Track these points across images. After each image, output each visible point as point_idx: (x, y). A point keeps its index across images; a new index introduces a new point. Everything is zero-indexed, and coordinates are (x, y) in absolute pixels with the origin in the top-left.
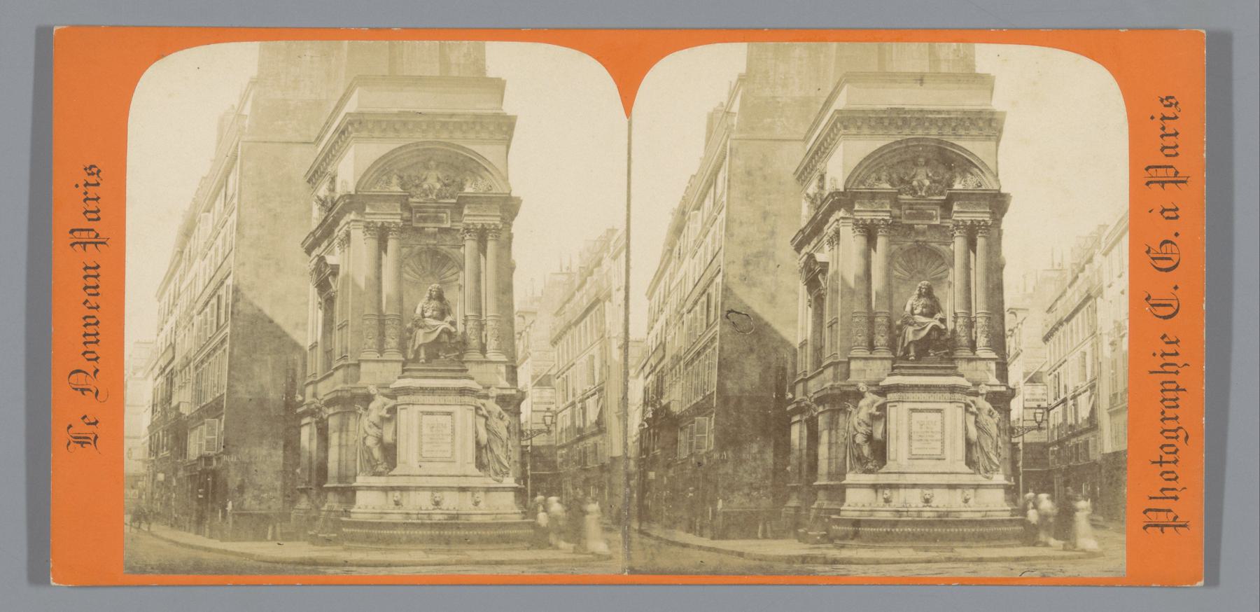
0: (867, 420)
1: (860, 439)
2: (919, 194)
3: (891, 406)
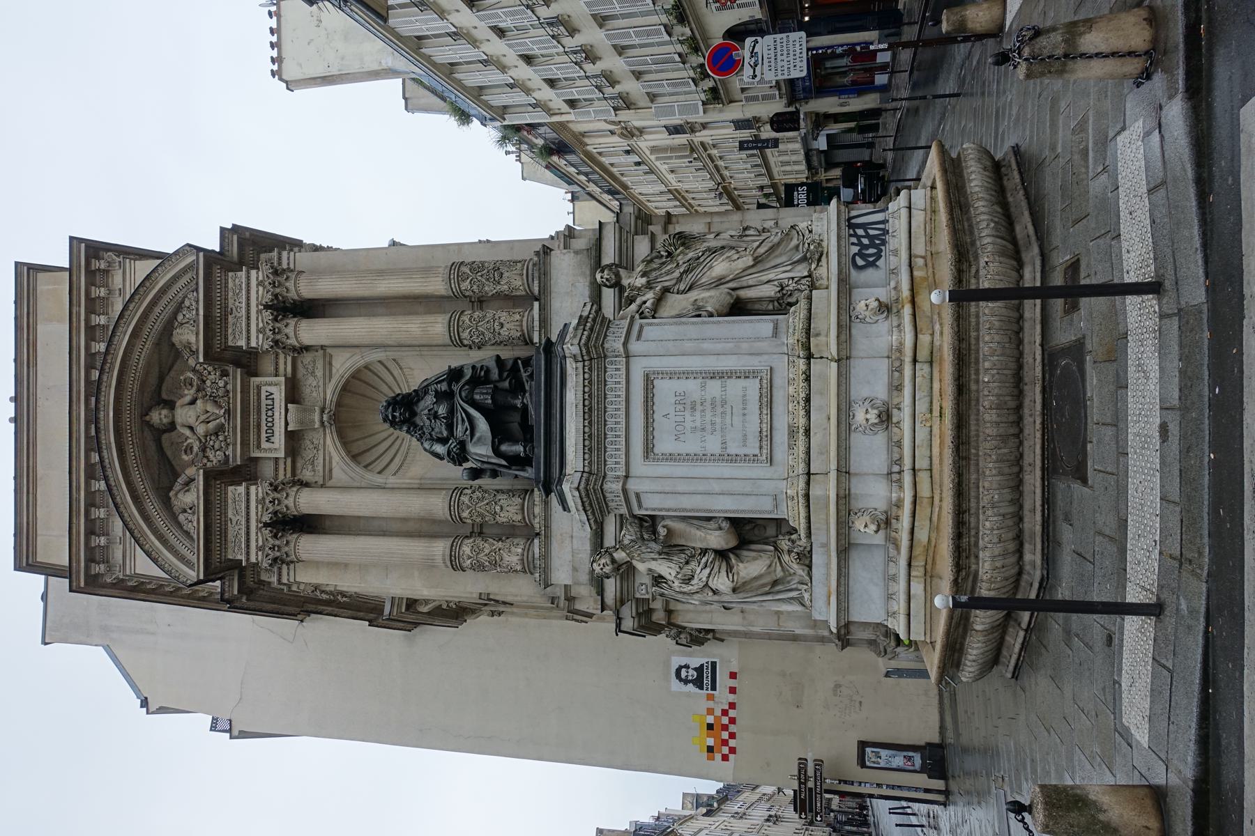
1: (722, 582)
2: (223, 421)
3: (640, 506)
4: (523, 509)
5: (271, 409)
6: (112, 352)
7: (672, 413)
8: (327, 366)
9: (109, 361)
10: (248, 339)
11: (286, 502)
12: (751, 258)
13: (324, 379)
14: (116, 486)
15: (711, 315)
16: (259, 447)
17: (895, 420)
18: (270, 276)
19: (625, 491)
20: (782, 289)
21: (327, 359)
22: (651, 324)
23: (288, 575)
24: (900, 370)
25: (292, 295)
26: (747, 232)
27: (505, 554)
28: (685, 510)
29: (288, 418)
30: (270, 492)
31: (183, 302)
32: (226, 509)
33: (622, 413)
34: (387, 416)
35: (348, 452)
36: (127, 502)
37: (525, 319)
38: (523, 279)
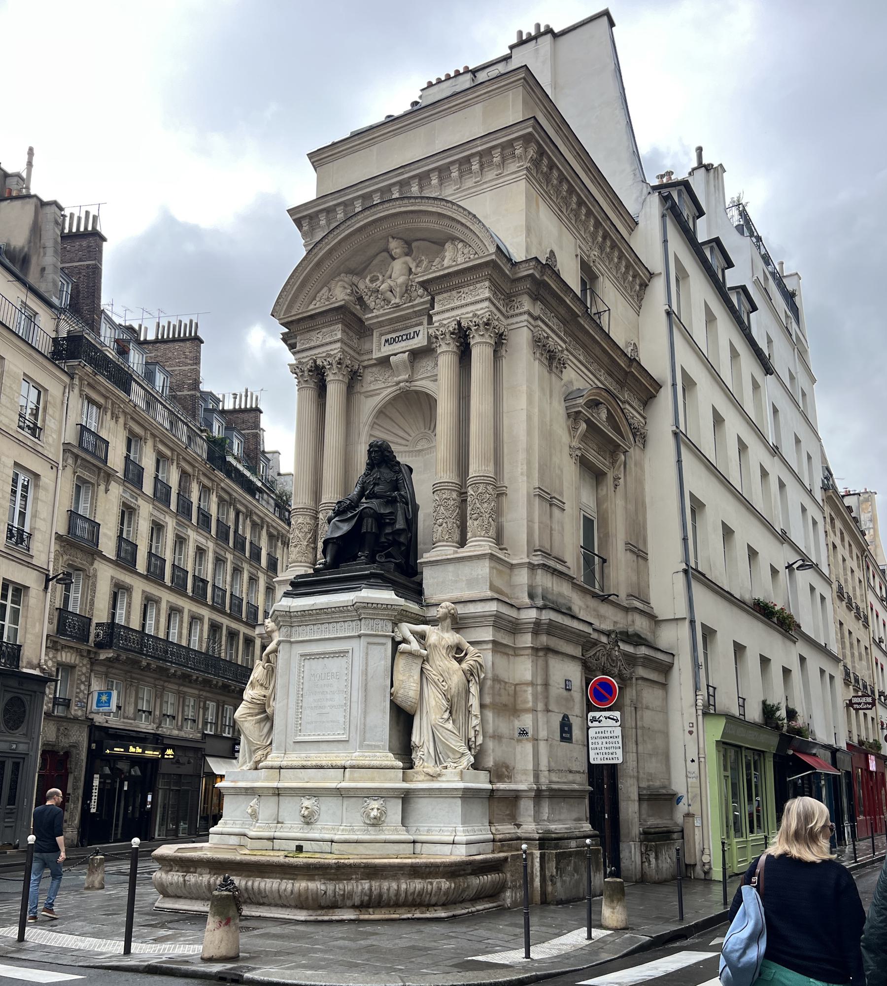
5: (407, 338)
11: (330, 374)
16: (382, 335)
32: (327, 326)
35: (385, 406)
37: (445, 543)
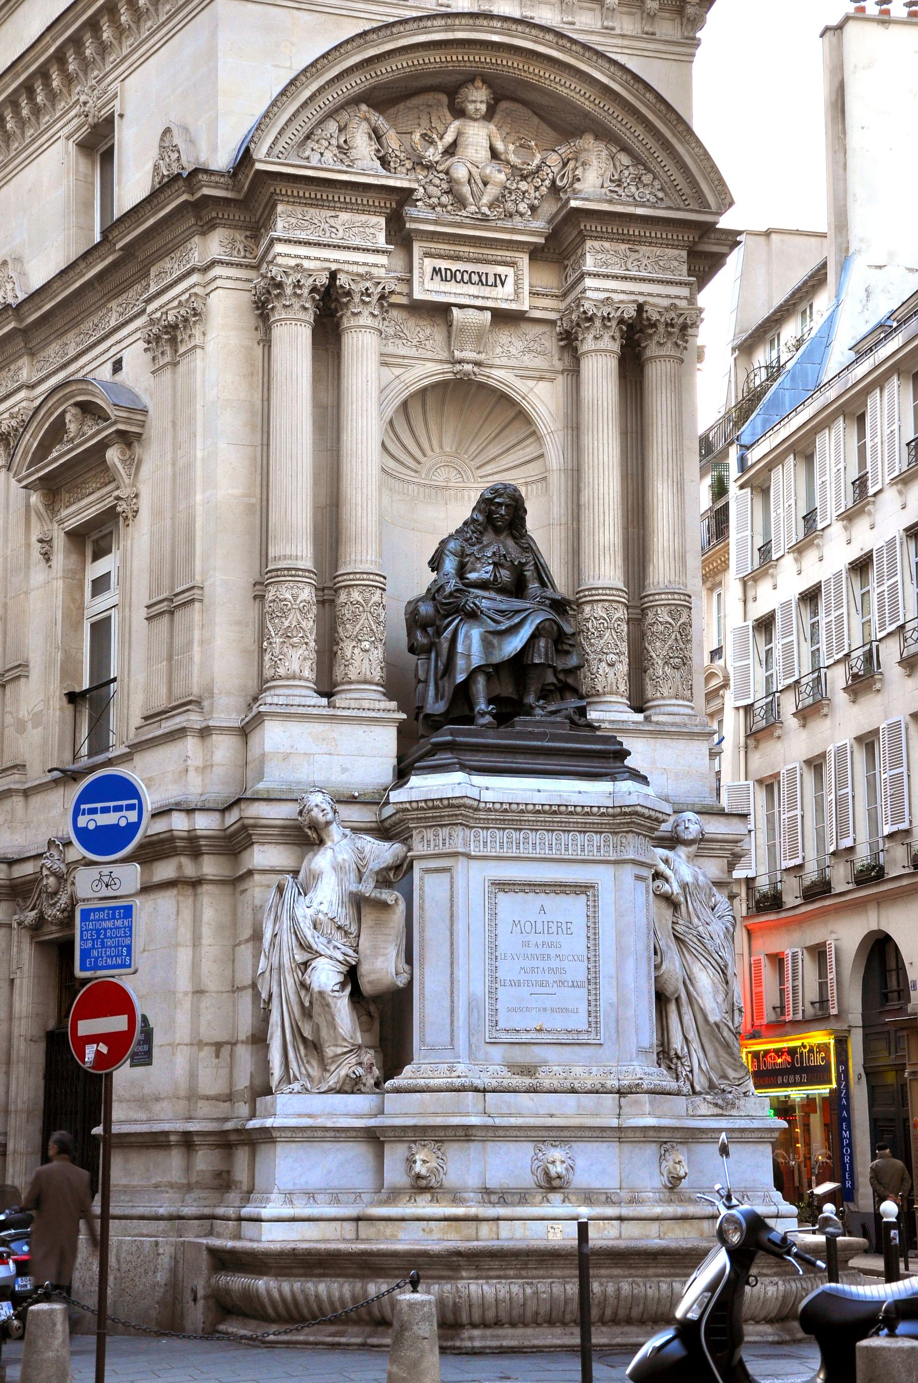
0: (344, 916)
2: (473, 208)
3: (428, 871)
4: (366, 682)
6: (587, 55)
7: (545, 918)
8: (537, 374)
9: (574, 48)
10: (596, 275)
11: (366, 313)
12: (717, 1019)
13: (520, 368)
14: (392, 34)
15: (657, 967)
16: (428, 255)
17: (551, 1196)
18: (681, 320)
19: (455, 855)
20: (678, 1058)
21: (548, 375)
22: (647, 892)
23: (228, 278)
24: (609, 1200)
25: (652, 350)
26: (736, 1012)
27: (301, 652)
28: (422, 931)
29: (471, 311)
30: (381, 287)
31: (648, 170)
33: (547, 853)
34: (500, 496)
36: (366, 49)
38: (670, 698)
